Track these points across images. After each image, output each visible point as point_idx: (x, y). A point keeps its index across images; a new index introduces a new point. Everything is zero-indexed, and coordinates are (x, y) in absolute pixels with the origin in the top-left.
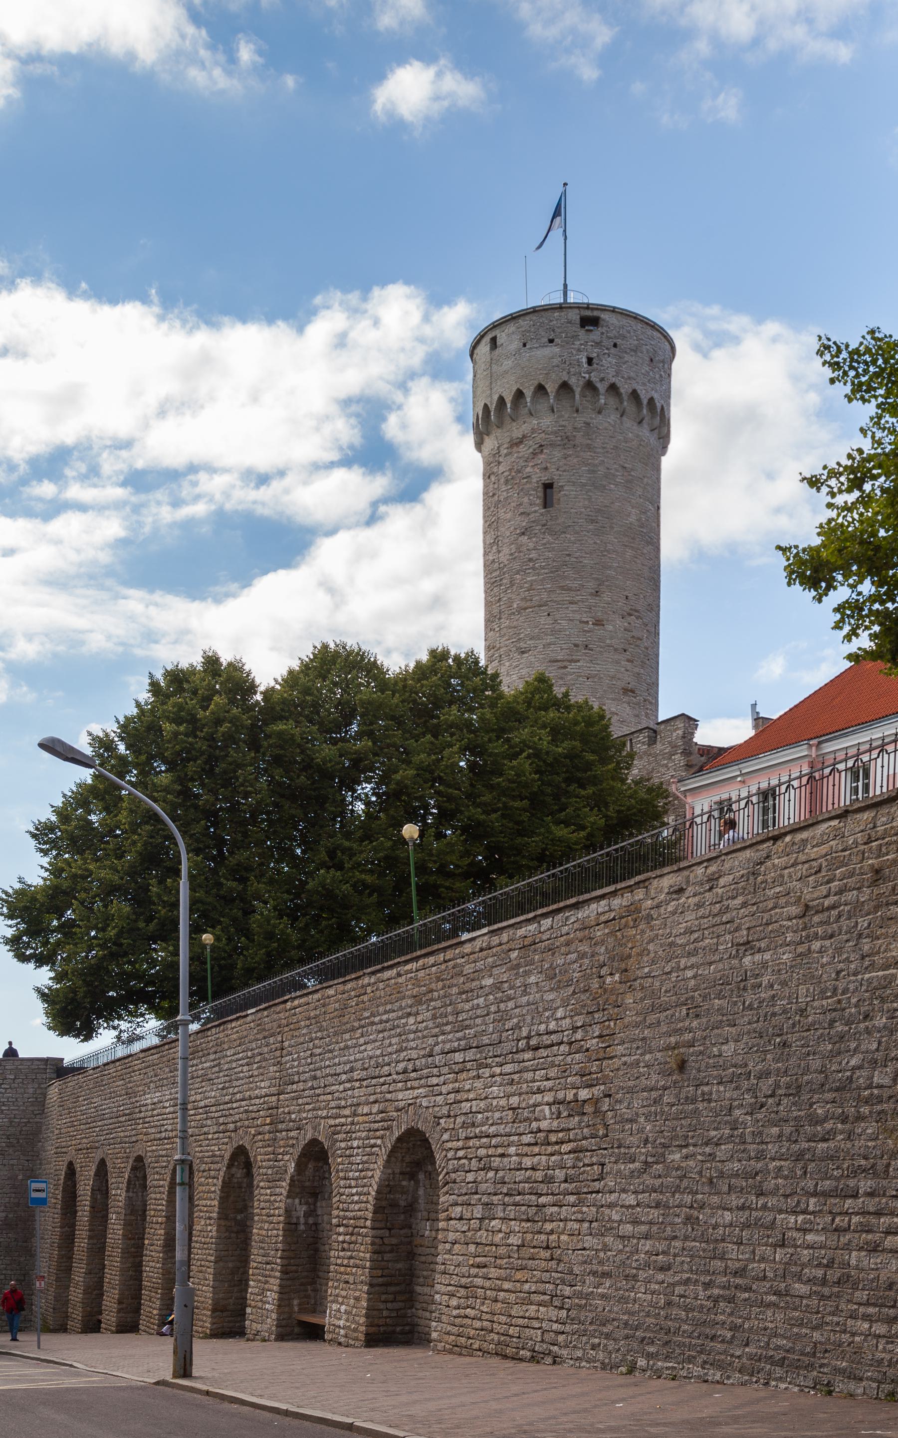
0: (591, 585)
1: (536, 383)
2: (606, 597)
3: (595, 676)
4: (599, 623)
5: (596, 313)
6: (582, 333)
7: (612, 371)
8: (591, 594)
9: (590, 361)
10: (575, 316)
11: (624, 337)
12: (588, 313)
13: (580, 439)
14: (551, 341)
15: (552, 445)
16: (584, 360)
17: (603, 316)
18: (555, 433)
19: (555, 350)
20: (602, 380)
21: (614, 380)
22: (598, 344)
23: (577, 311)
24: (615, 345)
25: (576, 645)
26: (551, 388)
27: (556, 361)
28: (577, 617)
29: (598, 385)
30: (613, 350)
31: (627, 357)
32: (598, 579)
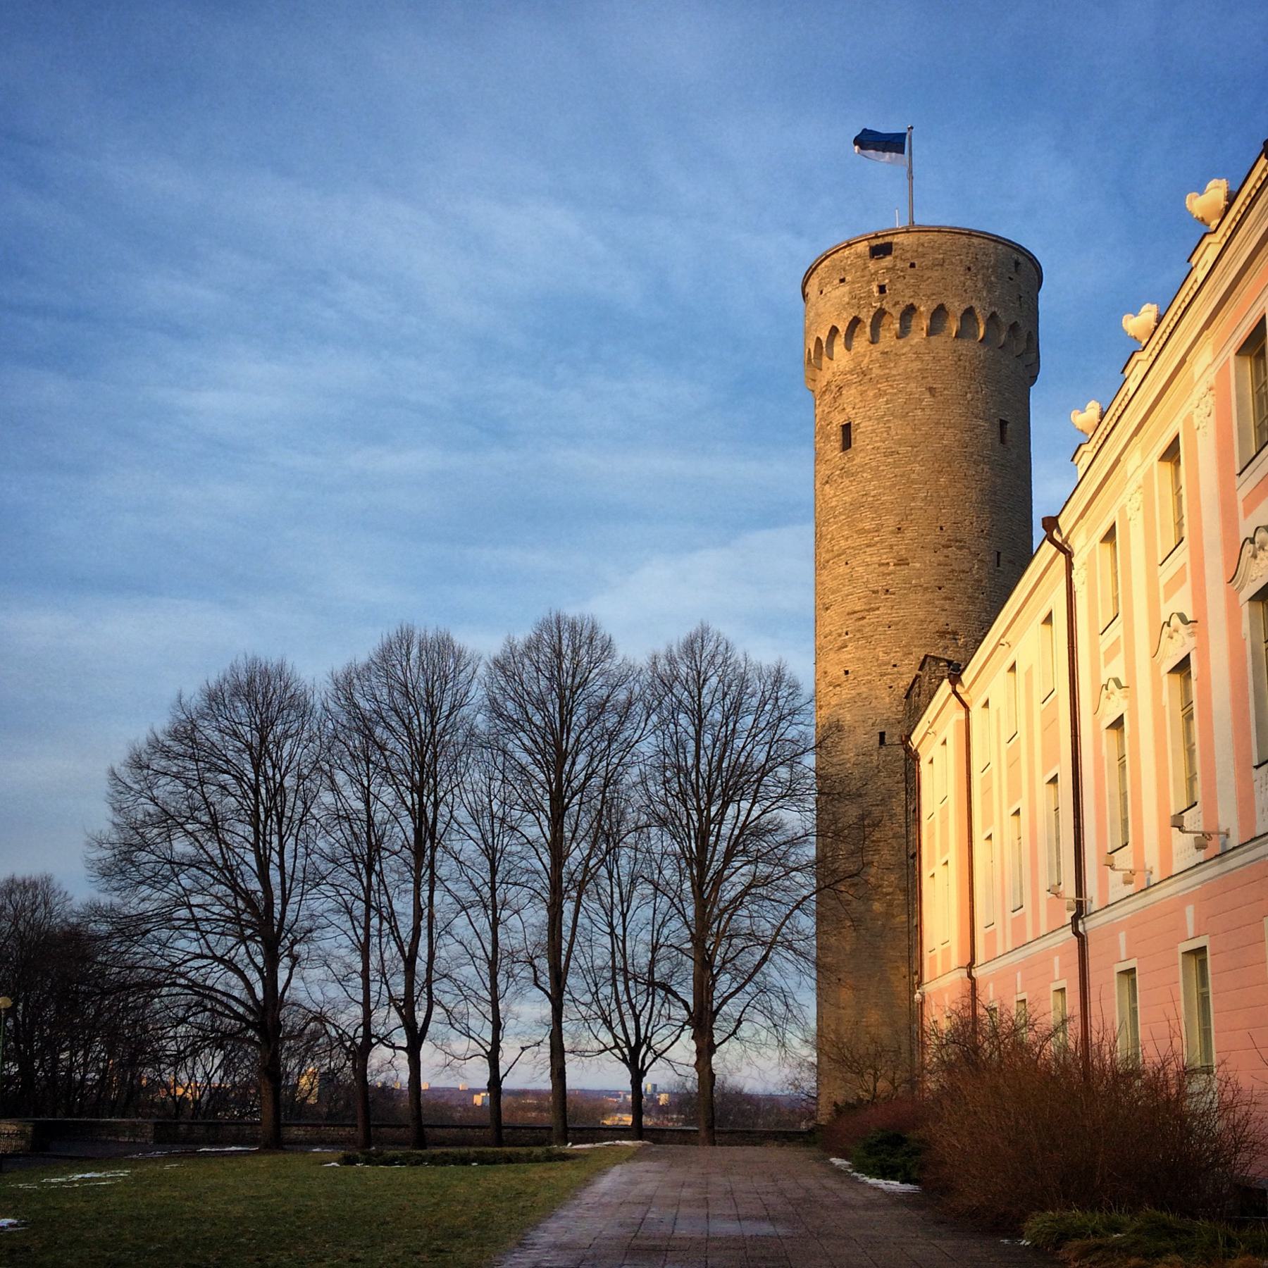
0: (891, 521)
1: (829, 327)
2: (909, 534)
3: (897, 624)
4: (902, 562)
5: (888, 239)
6: (872, 265)
7: (908, 292)
8: (892, 532)
9: (882, 289)
10: (863, 247)
11: (923, 255)
12: (880, 241)
13: (876, 371)
14: (842, 281)
15: (849, 384)
16: (875, 289)
17: (896, 239)
18: (851, 372)
19: (845, 289)
20: (897, 303)
21: (911, 300)
22: (888, 269)
23: (866, 243)
24: (912, 265)
25: (874, 592)
26: (842, 328)
27: (846, 299)
28: (875, 559)
29: (892, 311)
30: (910, 271)
31: (928, 273)
32: (897, 515)
